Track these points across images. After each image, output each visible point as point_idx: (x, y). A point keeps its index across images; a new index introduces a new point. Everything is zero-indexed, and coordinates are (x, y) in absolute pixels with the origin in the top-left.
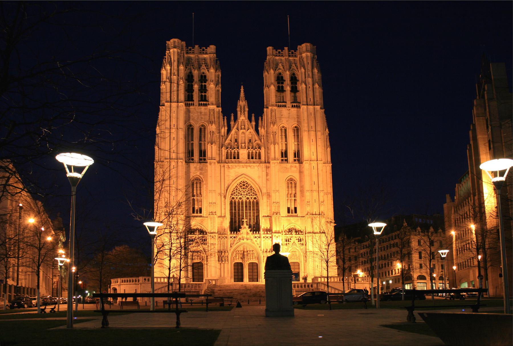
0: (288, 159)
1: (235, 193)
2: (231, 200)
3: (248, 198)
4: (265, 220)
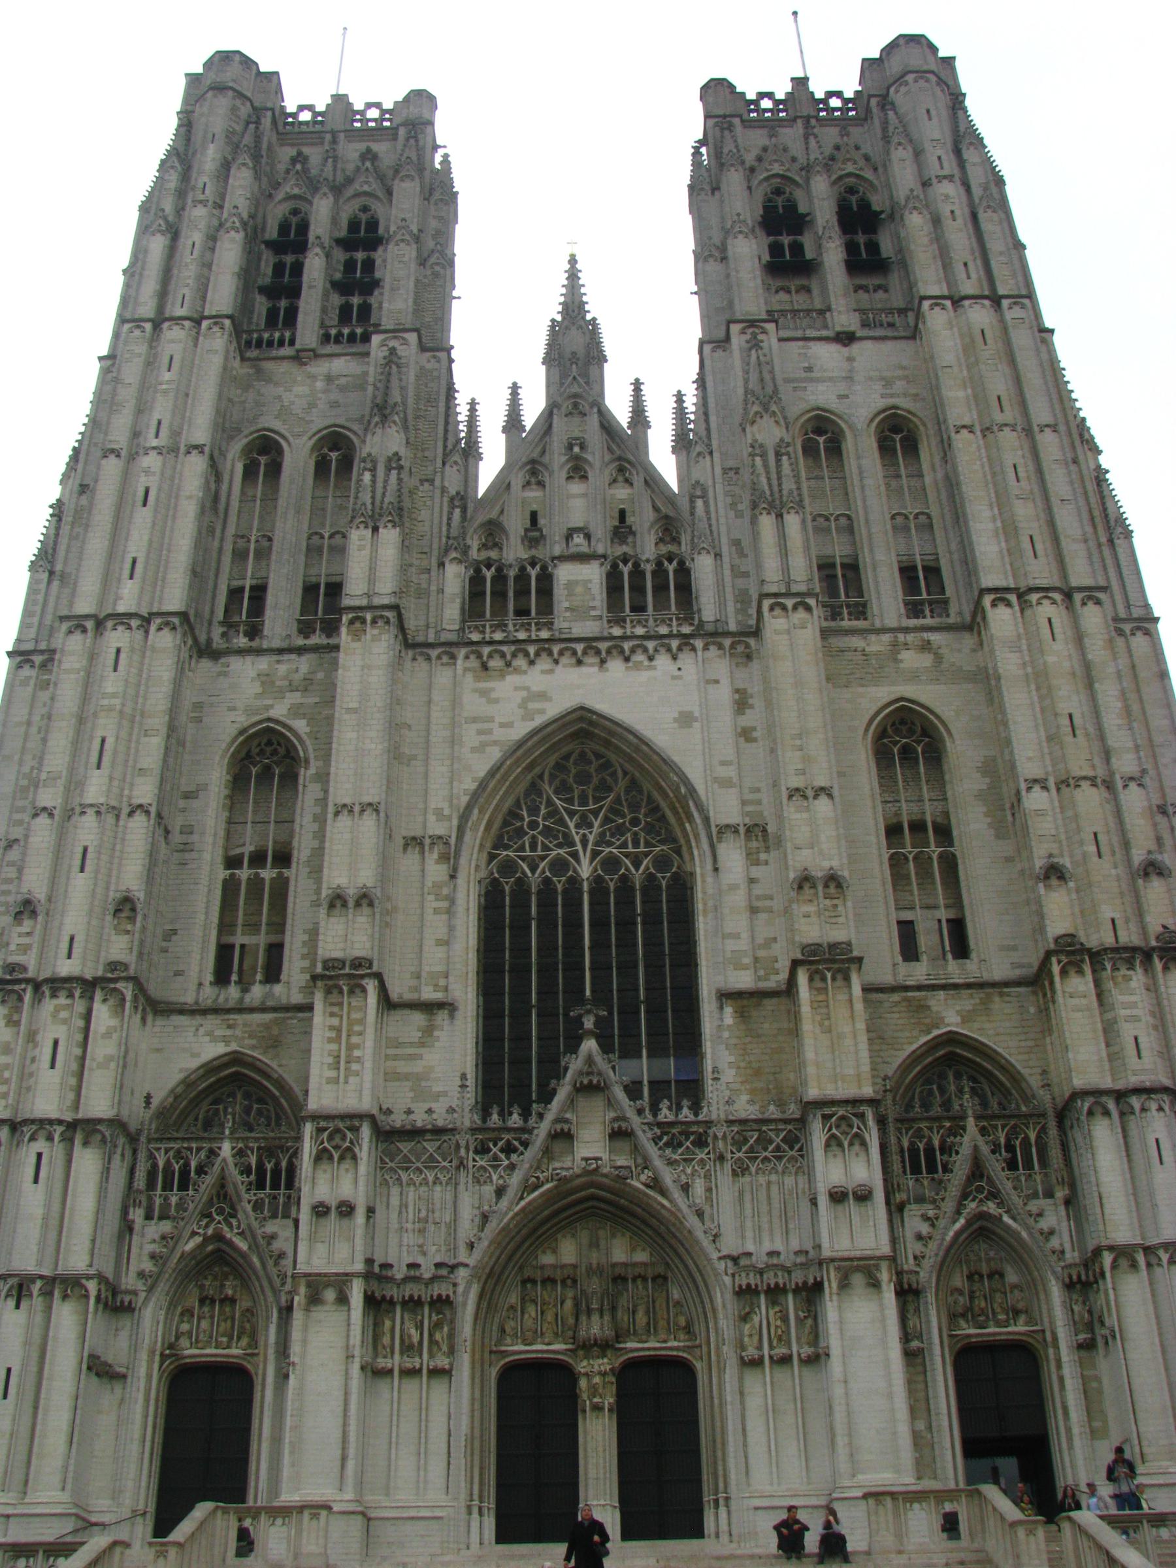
0: (864, 605)
1: (520, 832)
2: (495, 883)
3: (611, 864)
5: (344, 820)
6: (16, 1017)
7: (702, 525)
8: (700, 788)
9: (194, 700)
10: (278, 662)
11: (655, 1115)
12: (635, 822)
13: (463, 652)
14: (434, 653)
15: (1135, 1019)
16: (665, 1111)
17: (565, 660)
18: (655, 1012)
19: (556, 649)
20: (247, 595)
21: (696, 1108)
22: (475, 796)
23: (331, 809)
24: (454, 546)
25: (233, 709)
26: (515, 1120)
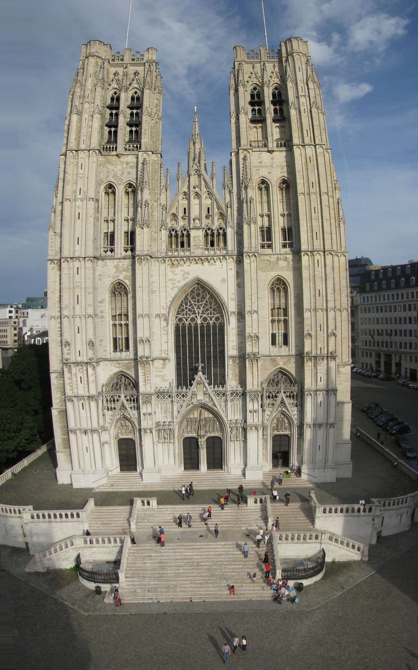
0: (272, 244)
1: (183, 310)
2: (178, 324)
3: (205, 319)
4: (234, 361)
5: (141, 318)
6: (70, 371)
7: (229, 217)
8: (227, 302)
9: (99, 273)
10: (120, 262)
11: (214, 388)
12: (211, 308)
13: (167, 259)
14: (160, 260)
15: (321, 373)
16: (216, 388)
17: (193, 262)
18: (215, 357)
19: (191, 259)
20: (109, 234)
21: (223, 387)
22: (172, 302)
23: (137, 316)
24: (163, 224)
25: (109, 276)
26: (184, 389)
